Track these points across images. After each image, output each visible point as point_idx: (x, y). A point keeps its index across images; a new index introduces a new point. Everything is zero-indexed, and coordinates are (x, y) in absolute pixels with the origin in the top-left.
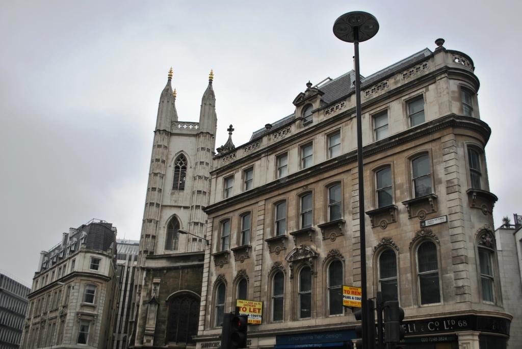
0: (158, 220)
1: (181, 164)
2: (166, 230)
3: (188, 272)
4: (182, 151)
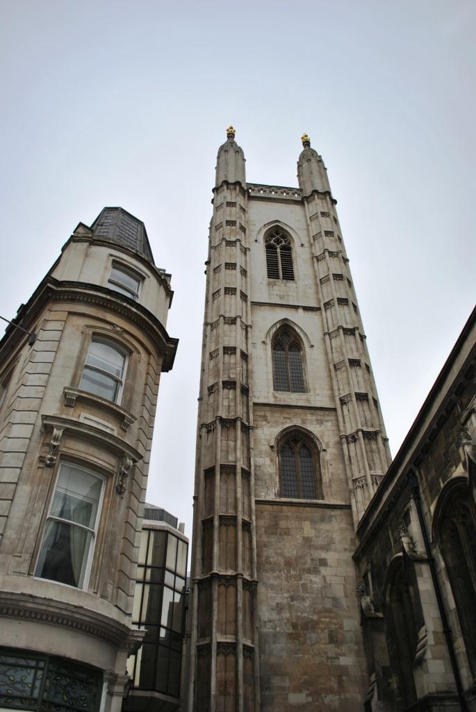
0: (249, 323)
2: (269, 347)
4: (277, 221)
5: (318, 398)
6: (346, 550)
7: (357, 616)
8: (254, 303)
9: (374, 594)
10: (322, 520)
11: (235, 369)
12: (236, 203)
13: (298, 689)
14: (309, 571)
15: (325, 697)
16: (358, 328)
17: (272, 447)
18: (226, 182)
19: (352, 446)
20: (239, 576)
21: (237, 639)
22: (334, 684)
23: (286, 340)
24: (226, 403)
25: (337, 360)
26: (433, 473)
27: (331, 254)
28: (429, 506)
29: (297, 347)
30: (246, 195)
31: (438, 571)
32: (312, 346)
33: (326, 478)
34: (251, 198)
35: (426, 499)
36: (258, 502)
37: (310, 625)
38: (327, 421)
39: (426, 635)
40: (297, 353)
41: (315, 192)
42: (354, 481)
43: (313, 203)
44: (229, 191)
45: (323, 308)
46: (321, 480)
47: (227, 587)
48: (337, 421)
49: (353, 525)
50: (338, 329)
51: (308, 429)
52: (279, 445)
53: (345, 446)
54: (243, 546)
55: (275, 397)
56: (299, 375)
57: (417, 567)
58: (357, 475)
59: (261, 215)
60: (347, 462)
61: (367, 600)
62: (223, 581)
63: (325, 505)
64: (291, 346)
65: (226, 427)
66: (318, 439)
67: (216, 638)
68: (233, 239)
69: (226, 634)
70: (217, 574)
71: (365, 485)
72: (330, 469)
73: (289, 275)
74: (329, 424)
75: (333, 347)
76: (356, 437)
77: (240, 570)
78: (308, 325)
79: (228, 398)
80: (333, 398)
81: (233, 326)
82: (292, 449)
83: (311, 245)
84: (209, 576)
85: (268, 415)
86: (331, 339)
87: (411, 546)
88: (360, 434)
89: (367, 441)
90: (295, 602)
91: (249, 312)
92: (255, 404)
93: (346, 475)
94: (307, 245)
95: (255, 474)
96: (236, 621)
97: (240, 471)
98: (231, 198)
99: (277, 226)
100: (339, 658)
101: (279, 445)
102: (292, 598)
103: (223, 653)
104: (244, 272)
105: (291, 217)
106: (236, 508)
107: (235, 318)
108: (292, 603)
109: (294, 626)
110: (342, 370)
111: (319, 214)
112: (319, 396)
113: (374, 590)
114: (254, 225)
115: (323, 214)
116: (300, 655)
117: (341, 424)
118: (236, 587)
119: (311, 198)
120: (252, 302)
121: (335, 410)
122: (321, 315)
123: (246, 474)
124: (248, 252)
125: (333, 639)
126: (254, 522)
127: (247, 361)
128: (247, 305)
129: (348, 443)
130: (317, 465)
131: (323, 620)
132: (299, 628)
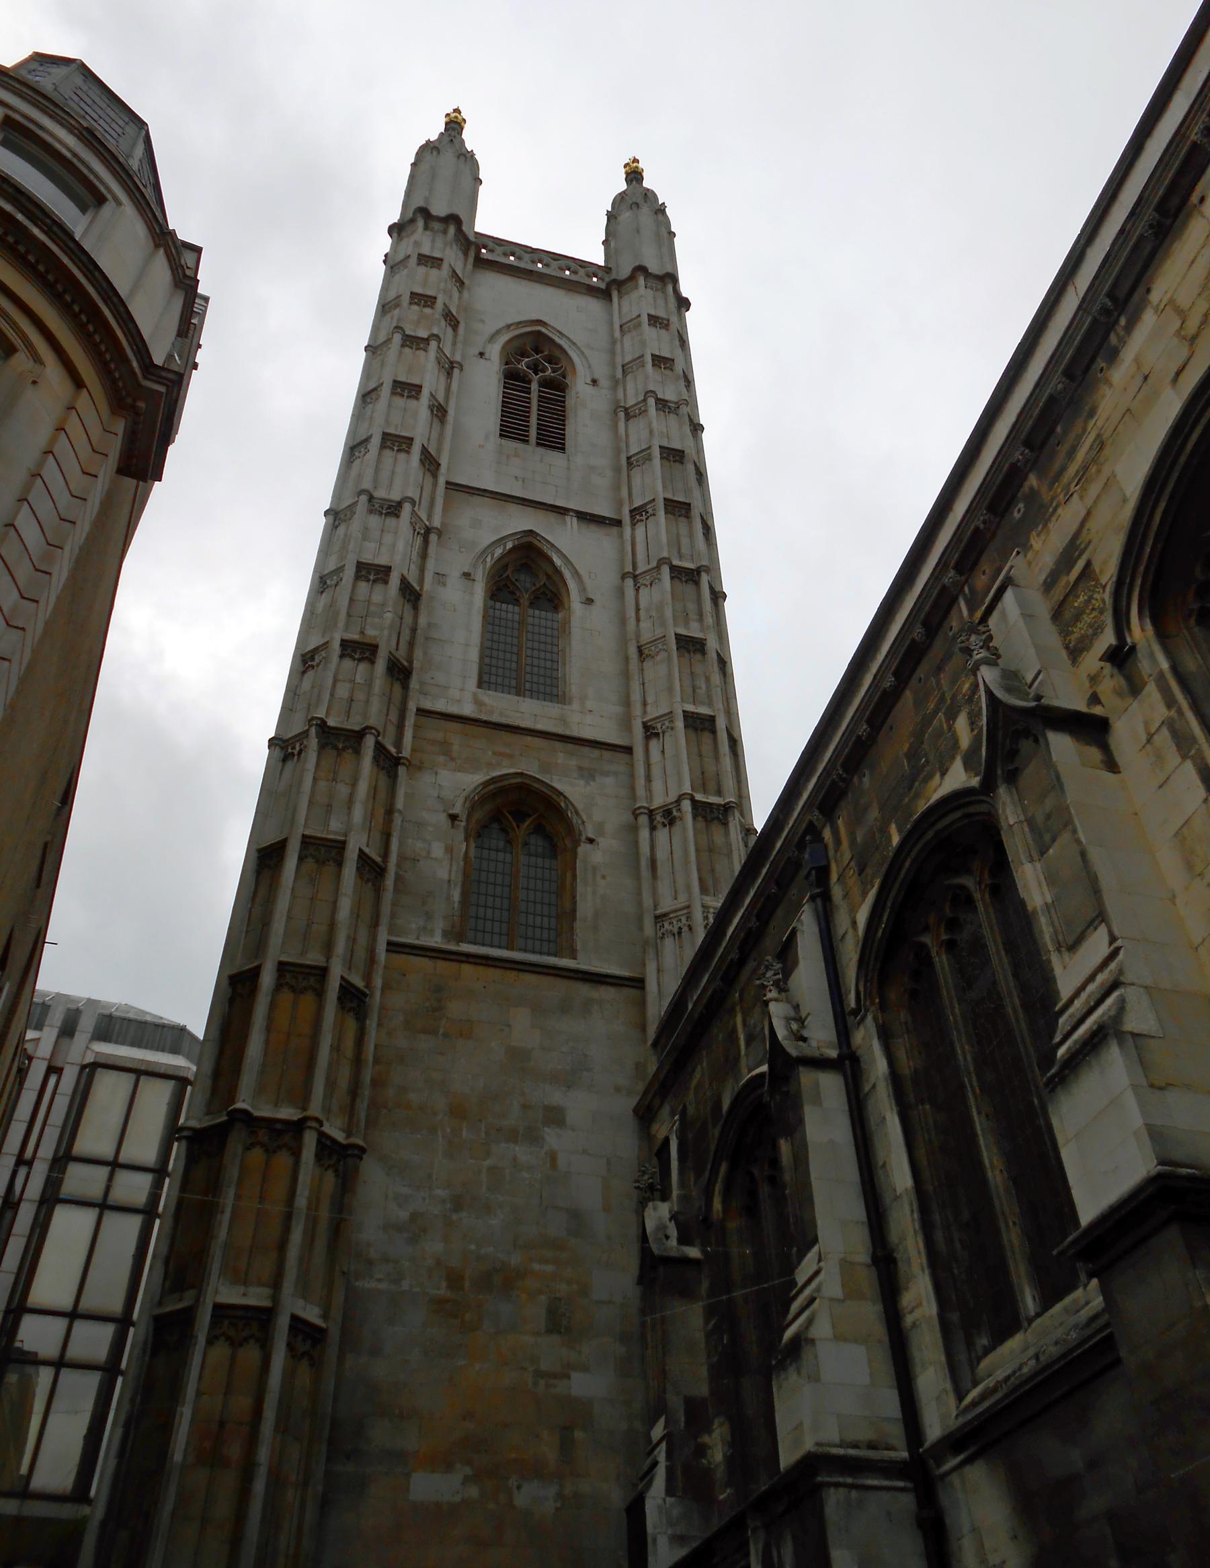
0: (437, 523)
5: (588, 719)
6: (618, 1089)
7: (632, 1264)
8: (451, 486)
9: (679, 1197)
10: (565, 1008)
11: (381, 617)
12: (442, 260)
13: (442, 1462)
14: (513, 1136)
15: (519, 1487)
16: (707, 570)
17: (453, 818)
18: (424, 212)
19: (662, 835)
20: (310, 1124)
21: (275, 1298)
22: (548, 1451)
23: (526, 579)
24: (343, 691)
25: (646, 637)
26: (874, 814)
27: (662, 404)
28: (853, 911)
29: (550, 600)
30: (472, 254)
31: (867, 1088)
32: (589, 601)
33: (586, 906)
34: (480, 263)
35: (846, 896)
36: (393, 947)
37: (500, 1280)
38: (606, 774)
39: (817, 1273)
40: (549, 615)
41: (641, 269)
42: (659, 918)
43: (634, 295)
44: (428, 233)
45: (627, 519)
46: (574, 911)
47: (270, 1151)
48: (632, 776)
49: (643, 1028)
50: (658, 567)
51: (554, 785)
52: (474, 820)
53: (644, 834)
54: (336, 1048)
55: (478, 702)
56: (549, 664)
57: (806, 1077)
58: (666, 905)
59: (503, 304)
60: (645, 872)
61: (659, 1213)
62: (263, 1135)
63: (577, 971)
64: (537, 598)
65: (336, 748)
66: (577, 813)
67: (216, 1292)
68: (423, 334)
69: (245, 1283)
70: (245, 1112)
71: (685, 929)
72: (600, 876)
73: (553, 438)
74: (610, 780)
75: (642, 606)
76: (675, 813)
77: (315, 1109)
78: (583, 555)
79: (353, 681)
80: (626, 723)
81: (391, 521)
82: (507, 833)
83: (615, 383)
84: (225, 1118)
85: (456, 743)
86: (637, 590)
87: (794, 1026)
88: (686, 805)
89: (701, 824)
90: (464, 1214)
91: (439, 501)
92: (421, 712)
93: (640, 903)
94: (604, 382)
95: (398, 879)
96: (282, 1246)
97: (355, 856)
98: (432, 248)
99: (539, 332)
100: (569, 1377)
101: (474, 820)
102: (458, 1204)
103: (228, 1338)
104: (439, 412)
105: (573, 320)
106: (328, 947)
107: (399, 504)
108: (455, 1217)
109: (454, 1279)
110: (658, 658)
111: (645, 319)
112: (594, 718)
113: (683, 1184)
114: (483, 321)
115: (654, 320)
116: (461, 1363)
117: (641, 782)
118: (296, 1153)
119: (630, 284)
120: (447, 483)
121: (628, 750)
122: (621, 536)
123: (372, 870)
124: (456, 371)
125: (557, 1322)
126: (378, 994)
127: (416, 608)
128: (435, 485)
129: (653, 828)
130: (569, 875)
131: (536, 1267)
132: (467, 1284)
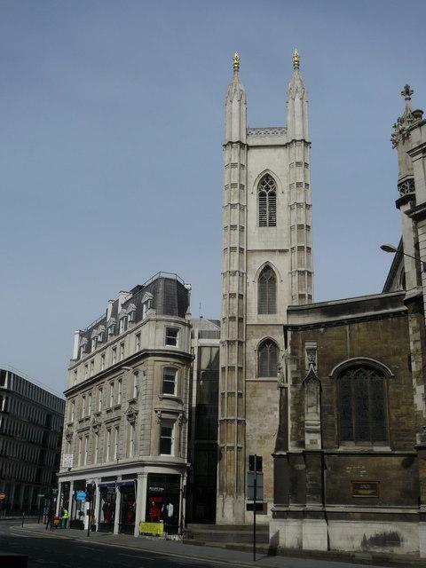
1: (267, 189)
2: (256, 284)
3: (359, 329)
23: (267, 277)
73: (273, 224)
78: (281, 265)
102: (261, 425)
